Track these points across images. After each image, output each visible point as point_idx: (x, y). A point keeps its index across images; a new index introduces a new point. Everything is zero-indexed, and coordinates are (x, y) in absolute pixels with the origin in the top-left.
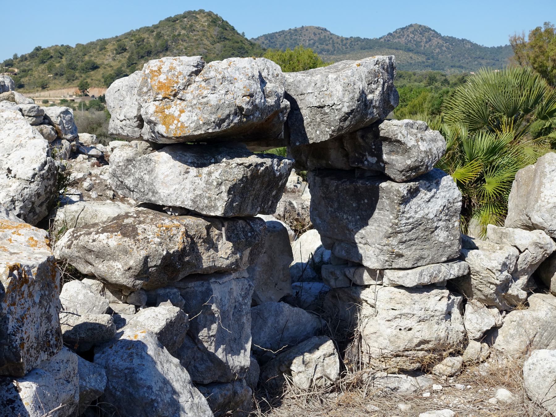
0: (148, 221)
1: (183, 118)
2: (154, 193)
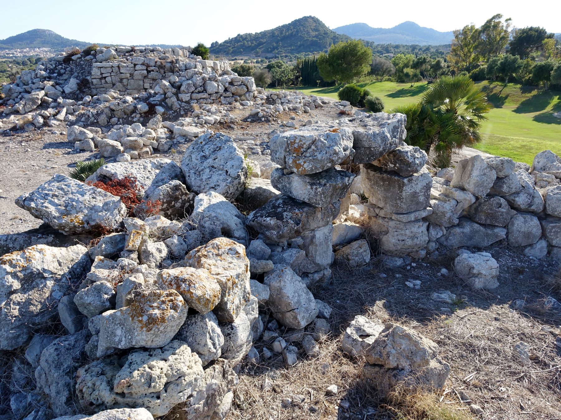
0: (288, 210)
1: (305, 165)
2: (291, 193)
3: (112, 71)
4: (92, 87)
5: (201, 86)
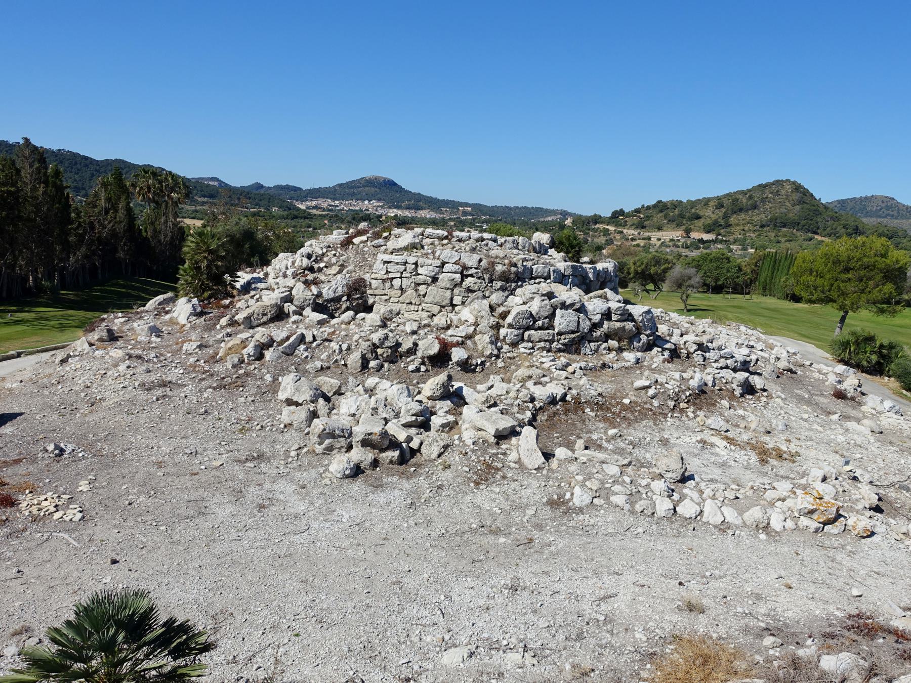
3: (405, 270)
4: (368, 292)
5: (545, 318)
